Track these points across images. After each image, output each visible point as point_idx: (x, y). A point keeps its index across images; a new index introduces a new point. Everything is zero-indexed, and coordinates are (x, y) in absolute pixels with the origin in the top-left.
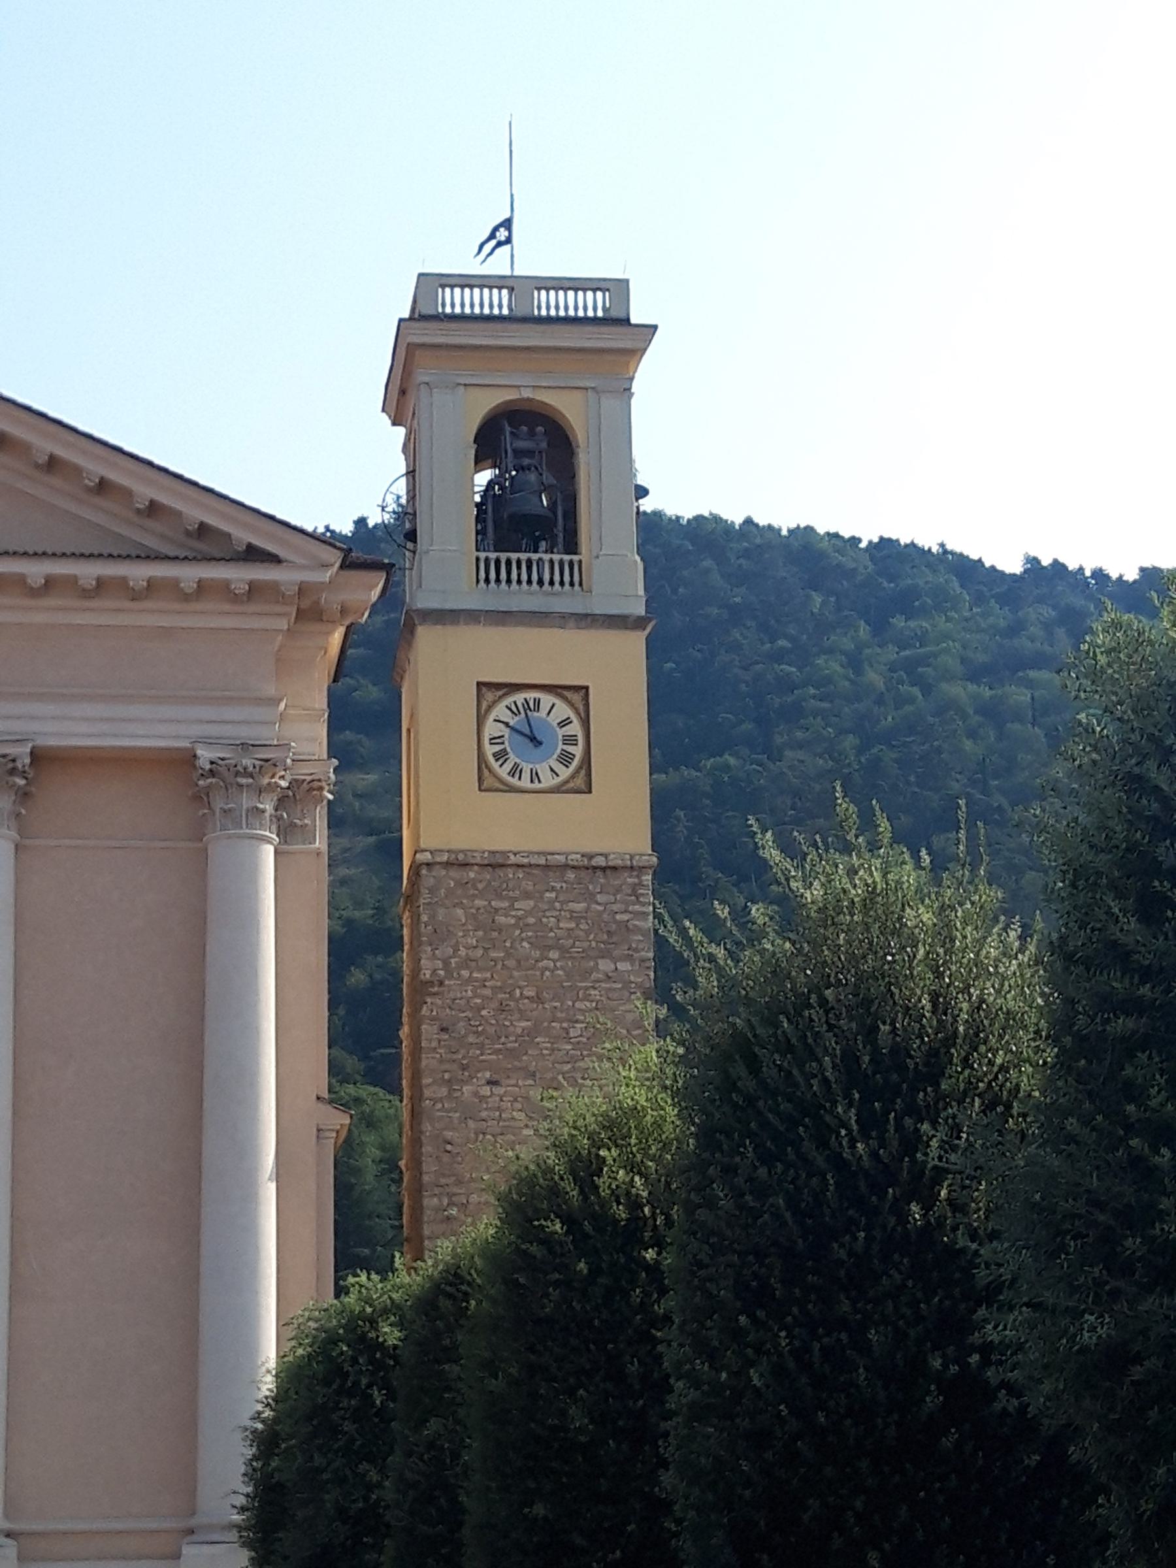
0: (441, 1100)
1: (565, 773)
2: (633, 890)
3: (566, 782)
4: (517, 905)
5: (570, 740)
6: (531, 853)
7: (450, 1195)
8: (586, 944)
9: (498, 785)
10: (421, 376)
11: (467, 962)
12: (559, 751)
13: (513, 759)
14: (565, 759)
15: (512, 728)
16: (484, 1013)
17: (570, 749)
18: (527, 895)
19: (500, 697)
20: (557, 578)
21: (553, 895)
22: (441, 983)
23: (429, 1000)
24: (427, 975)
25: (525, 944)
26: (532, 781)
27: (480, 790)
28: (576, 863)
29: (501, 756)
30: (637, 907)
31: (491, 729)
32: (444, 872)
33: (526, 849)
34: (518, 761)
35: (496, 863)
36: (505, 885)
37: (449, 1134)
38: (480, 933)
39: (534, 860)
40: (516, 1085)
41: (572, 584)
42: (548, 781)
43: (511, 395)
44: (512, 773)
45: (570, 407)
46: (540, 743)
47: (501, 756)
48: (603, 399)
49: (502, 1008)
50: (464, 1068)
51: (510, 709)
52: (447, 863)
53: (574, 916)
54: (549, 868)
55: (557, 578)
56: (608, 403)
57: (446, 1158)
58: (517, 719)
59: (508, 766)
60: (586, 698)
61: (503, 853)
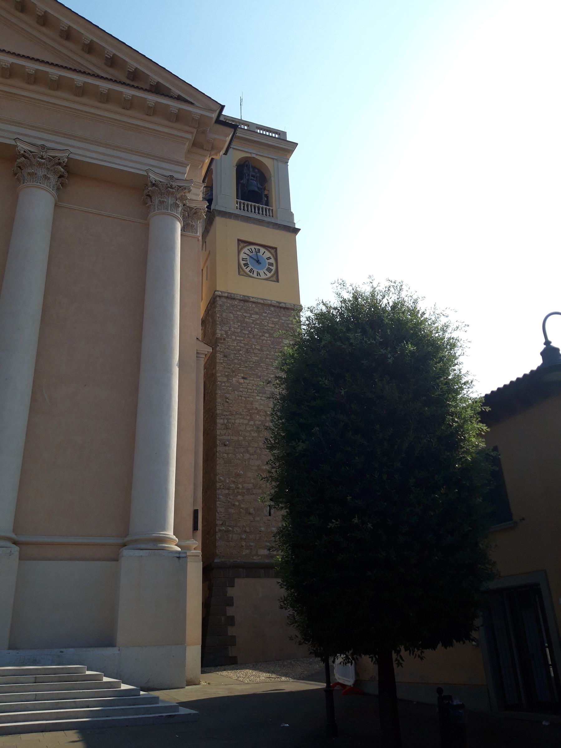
0: (224, 382)
1: (269, 275)
4: (253, 316)
5: (271, 264)
6: (258, 298)
7: (228, 419)
11: (234, 333)
13: (250, 267)
14: (269, 270)
15: (250, 257)
17: (271, 267)
18: (256, 313)
20: (264, 213)
21: (266, 315)
22: (224, 339)
25: (256, 330)
29: (246, 265)
31: (242, 255)
32: (225, 300)
35: (245, 300)
37: (228, 395)
38: (239, 324)
39: (260, 301)
40: (253, 380)
42: (263, 276)
44: (250, 271)
47: (246, 265)
49: (247, 351)
50: (233, 372)
54: (265, 305)
57: (226, 404)
59: (249, 269)
60: (276, 251)
61: (248, 297)
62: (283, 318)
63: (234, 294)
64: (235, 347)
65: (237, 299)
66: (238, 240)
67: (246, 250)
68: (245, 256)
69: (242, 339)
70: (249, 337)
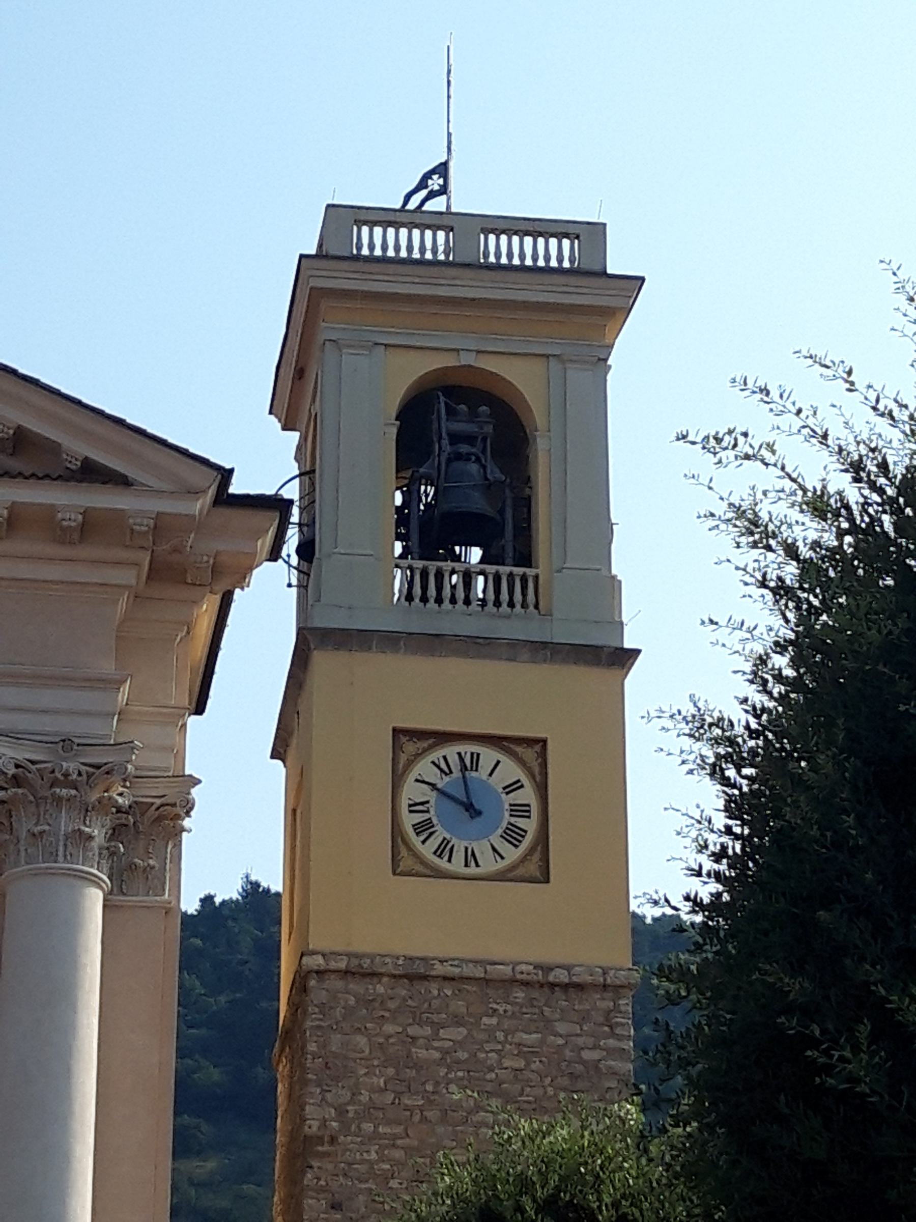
1: (512, 854)
2: (607, 1019)
3: (513, 867)
5: (521, 810)
8: (540, 1091)
9: (419, 868)
10: (326, 330)
12: (504, 824)
13: (441, 833)
14: (513, 835)
16: (394, 1184)
17: (521, 823)
18: (458, 1021)
19: (425, 751)
20: (504, 596)
21: (494, 1021)
22: (333, 1140)
23: (315, 1164)
24: (312, 1127)
25: (453, 1088)
26: (466, 865)
27: (394, 873)
28: (524, 977)
29: (424, 828)
30: (612, 1042)
31: (411, 791)
32: (339, 984)
33: (460, 956)
34: (448, 836)
35: (415, 974)
36: (426, 1005)
38: (391, 1071)
39: (469, 970)
41: (524, 605)
42: (488, 864)
43: (449, 361)
45: (523, 378)
46: (479, 813)
47: (424, 828)
48: (569, 373)
51: (438, 767)
52: (346, 972)
53: (522, 1050)
54: (489, 983)
55: (504, 596)
56: (577, 376)
58: (447, 779)
59: (434, 843)
62: (561, 1028)
63: (372, 957)
64: (371, 1163)
65: (382, 974)
66: (395, 731)
67: (425, 768)
68: (420, 793)
69: (399, 1130)
70: (424, 1119)
